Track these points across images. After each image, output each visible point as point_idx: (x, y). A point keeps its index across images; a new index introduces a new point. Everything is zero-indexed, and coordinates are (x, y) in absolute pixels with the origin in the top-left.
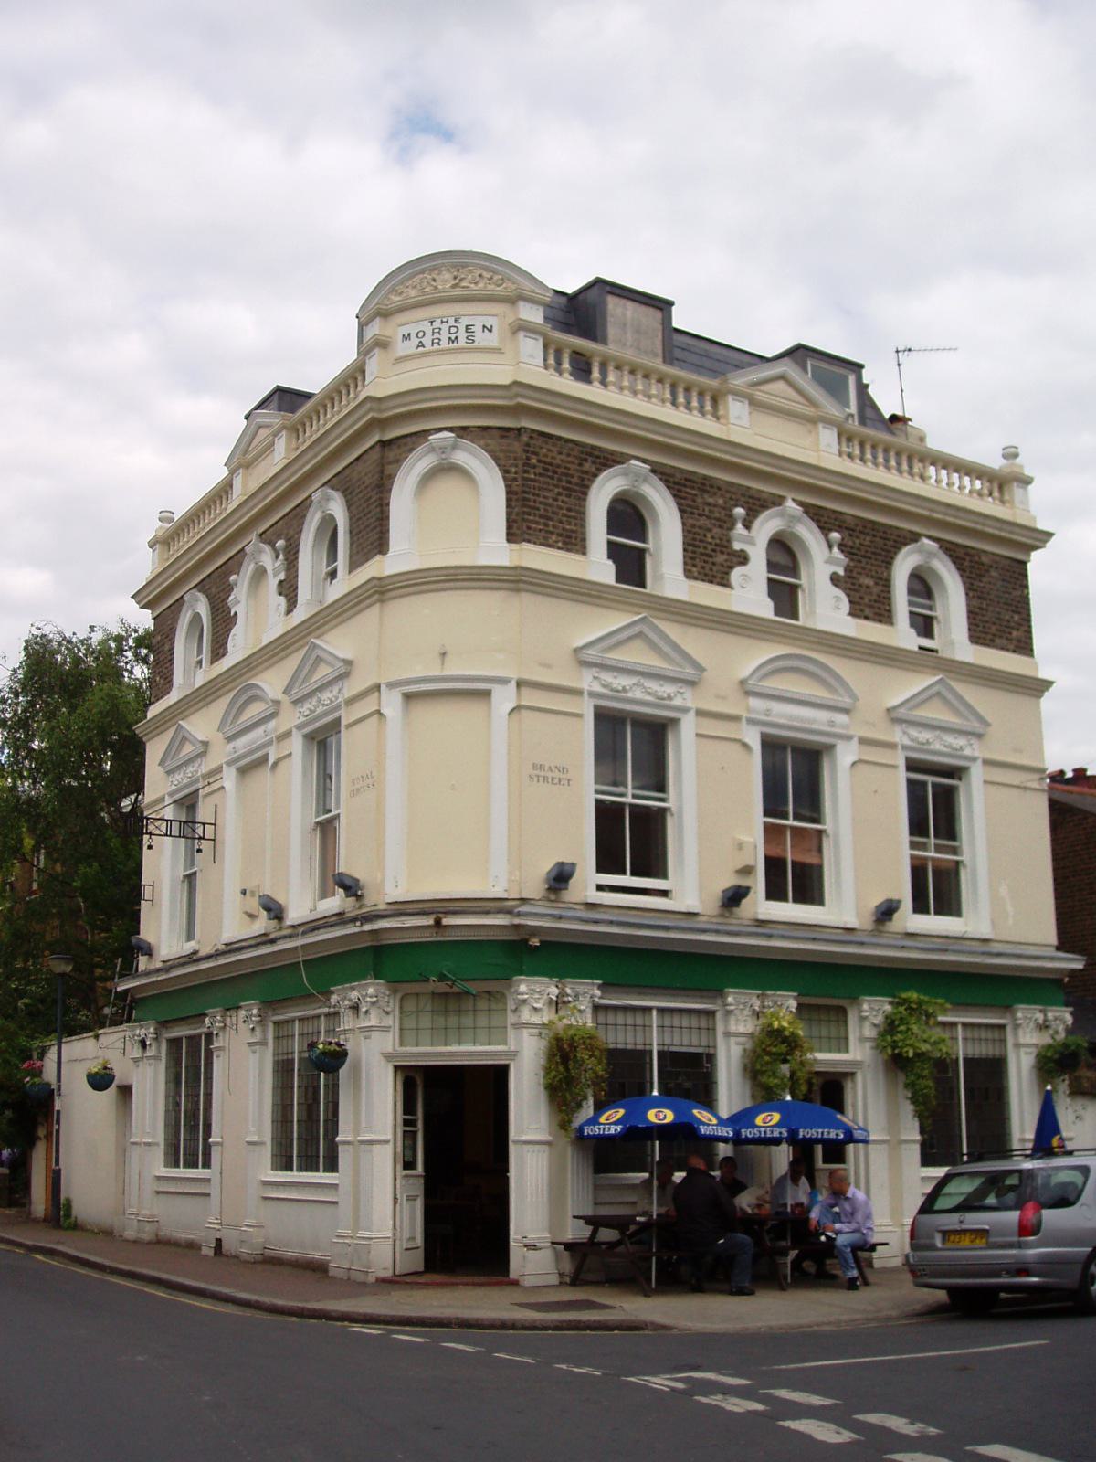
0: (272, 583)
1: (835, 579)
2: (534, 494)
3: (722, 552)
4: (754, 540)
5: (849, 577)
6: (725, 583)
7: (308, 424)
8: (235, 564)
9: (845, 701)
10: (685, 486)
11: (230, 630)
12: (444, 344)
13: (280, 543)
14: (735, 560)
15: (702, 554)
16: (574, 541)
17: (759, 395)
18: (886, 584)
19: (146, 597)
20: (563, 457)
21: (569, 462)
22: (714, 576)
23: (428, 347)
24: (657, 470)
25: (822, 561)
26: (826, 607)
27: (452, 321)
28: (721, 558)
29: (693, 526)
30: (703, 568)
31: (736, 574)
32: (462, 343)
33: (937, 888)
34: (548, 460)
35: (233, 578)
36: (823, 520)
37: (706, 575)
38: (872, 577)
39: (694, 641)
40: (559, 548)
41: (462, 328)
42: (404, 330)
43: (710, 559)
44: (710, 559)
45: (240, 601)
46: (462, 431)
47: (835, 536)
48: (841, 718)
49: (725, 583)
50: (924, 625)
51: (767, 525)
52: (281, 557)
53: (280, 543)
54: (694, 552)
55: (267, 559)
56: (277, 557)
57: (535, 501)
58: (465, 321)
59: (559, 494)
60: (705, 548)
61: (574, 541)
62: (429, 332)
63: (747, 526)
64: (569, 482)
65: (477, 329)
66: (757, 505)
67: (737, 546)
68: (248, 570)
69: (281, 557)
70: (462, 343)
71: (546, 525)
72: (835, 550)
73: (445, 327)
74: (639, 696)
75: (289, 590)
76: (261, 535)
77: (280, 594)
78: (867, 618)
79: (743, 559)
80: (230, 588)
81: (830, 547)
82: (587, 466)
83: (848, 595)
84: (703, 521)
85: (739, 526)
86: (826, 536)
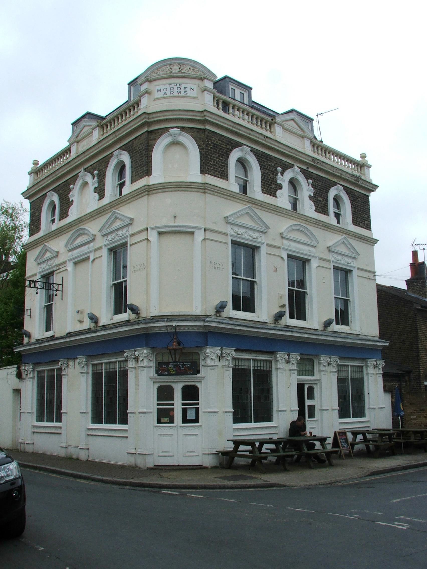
0: (91, 188)
1: (310, 197)
2: (210, 155)
3: (274, 184)
4: (283, 180)
5: (315, 197)
6: (275, 196)
7: (112, 122)
8: (73, 180)
9: (314, 243)
10: (261, 157)
11: (70, 207)
12: (175, 94)
13: (96, 172)
14: (278, 187)
15: (267, 184)
16: (224, 175)
17: (286, 126)
18: (326, 200)
19: (27, 195)
20: (220, 142)
21: (222, 144)
22: (271, 193)
23: (168, 95)
24: (253, 151)
25: (306, 190)
26: (308, 208)
27: (178, 85)
28: (273, 186)
29: (264, 173)
30: (267, 189)
31: (279, 192)
32: (182, 94)
33: (343, 316)
34: (215, 142)
35: (71, 186)
36: (307, 175)
37: (268, 192)
38: (322, 197)
39: (268, 218)
40: (219, 177)
41: (182, 88)
42: (158, 88)
43: (270, 187)
44: (270, 187)
45: (74, 195)
46: (183, 129)
47: (310, 181)
48: (313, 250)
49: (275, 196)
50: (337, 216)
51: (289, 174)
52: (96, 178)
53: (96, 172)
54: (264, 183)
55: (89, 178)
56: (94, 178)
57: (210, 158)
58: (183, 86)
59: (219, 156)
60: (268, 182)
61: (224, 175)
62: (169, 89)
63: (282, 174)
64: (222, 152)
65: (189, 89)
66: (286, 167)
67: (279, 182)
68: (79, 183)
69: (96, 178)
70: (182, 94)
71: (214, 168)
72: (310, 186)
73: (175, 88)
74: (247, 237)
75: (100, 191)
76: (85, 169)
77: (95, 192)
78: (320, 213)
79: (280, 187)
80: (70, 190)
81: (309, 185)
82: (228, 146)
83: (314, 204)
84: (267, 171)
85: (279, 174)
86: (307, 181)
